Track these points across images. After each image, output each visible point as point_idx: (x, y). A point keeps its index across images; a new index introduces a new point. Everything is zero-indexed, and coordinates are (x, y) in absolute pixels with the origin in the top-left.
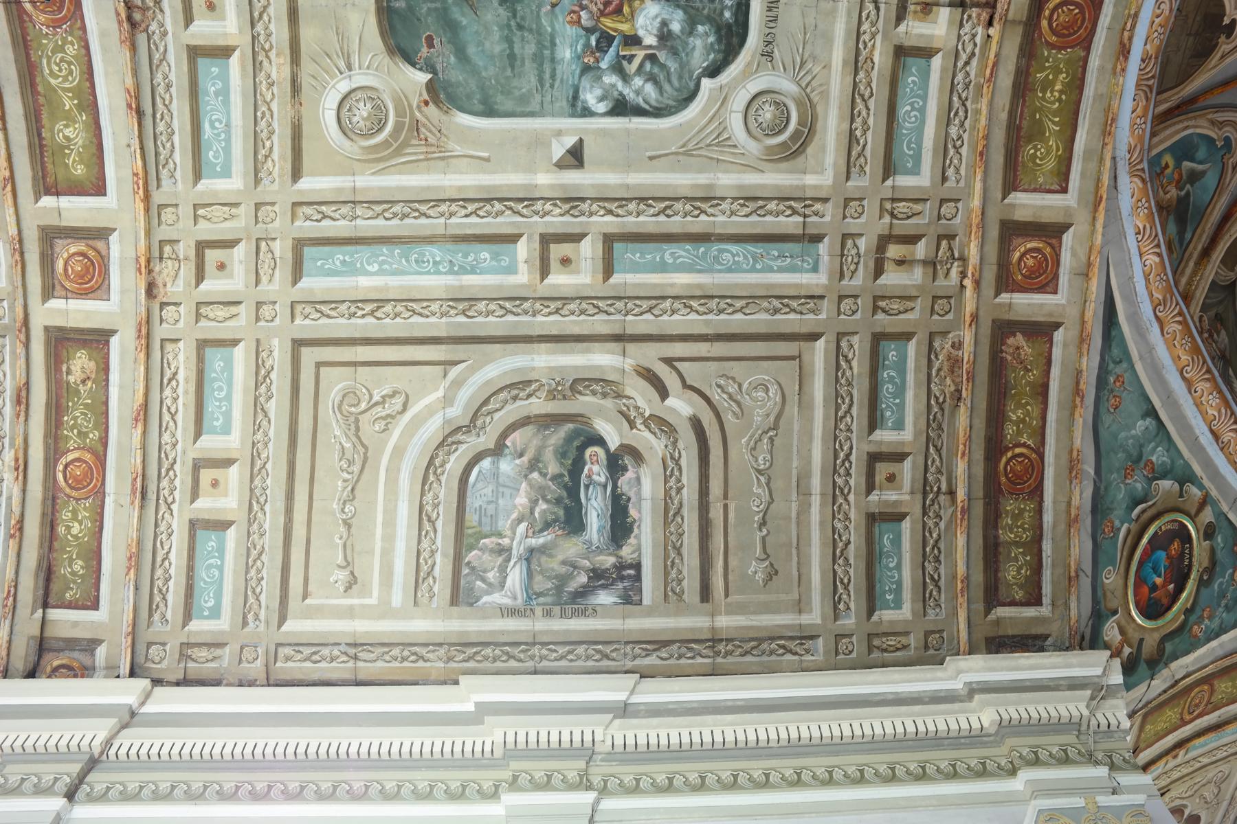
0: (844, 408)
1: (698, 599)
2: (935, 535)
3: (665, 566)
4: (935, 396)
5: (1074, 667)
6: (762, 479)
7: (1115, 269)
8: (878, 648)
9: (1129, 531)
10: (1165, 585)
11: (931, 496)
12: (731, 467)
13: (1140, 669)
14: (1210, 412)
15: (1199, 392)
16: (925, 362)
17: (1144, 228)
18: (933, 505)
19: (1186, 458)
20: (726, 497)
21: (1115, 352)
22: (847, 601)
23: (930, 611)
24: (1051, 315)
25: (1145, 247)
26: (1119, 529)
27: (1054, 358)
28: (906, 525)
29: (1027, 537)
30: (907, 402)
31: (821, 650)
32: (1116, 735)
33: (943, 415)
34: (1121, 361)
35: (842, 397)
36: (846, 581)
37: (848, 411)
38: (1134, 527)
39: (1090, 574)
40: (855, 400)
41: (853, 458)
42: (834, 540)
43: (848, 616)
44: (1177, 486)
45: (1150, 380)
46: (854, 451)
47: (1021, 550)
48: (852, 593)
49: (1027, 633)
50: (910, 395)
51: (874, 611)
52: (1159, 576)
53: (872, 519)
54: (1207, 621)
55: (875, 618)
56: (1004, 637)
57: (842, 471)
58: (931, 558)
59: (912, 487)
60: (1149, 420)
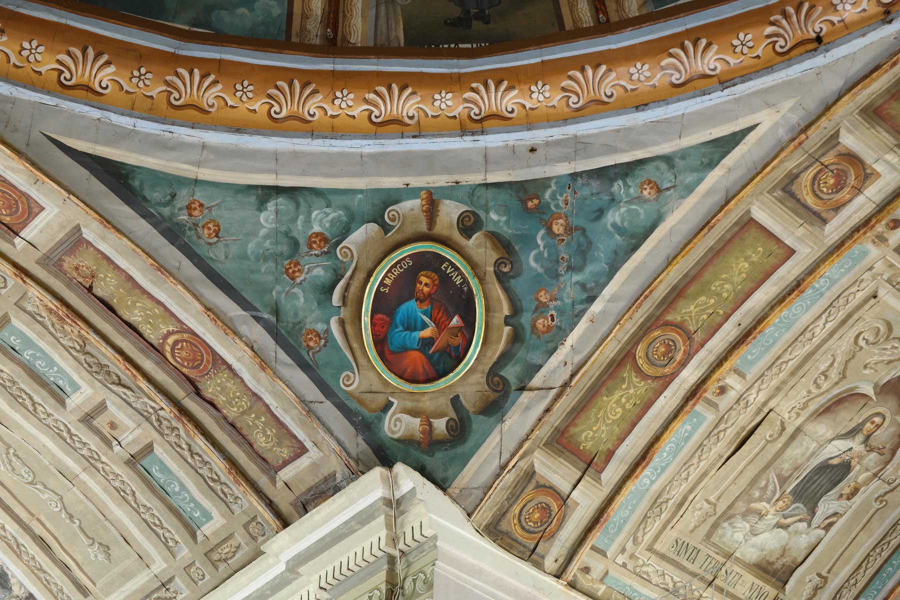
0: (28, 402)
1: (81, 597)
2: (184, 446)
3: (45, 585)
4: (72, 348)
5: (359, 500)
6: (38, 486)
7: (70, 136)
8: (220, 560)
9: (342, 323)
10: (440, 326)
11: (153, 418)
12: (15, 492)
13: (475, 426)
14: (355, 112)
15: (319, 114)
16: (38, 326)
17: (59, 62)
18: (161, 423)
19: (363, 187)
20: (32, 515)
21: (155, 195)
22: (172, 537)
23: (234, 507)
24: (62, 227)
25: (83, 75)
26: (328, 331)
27: (108, 254)
28: (158, 450)
29: (246, 403)
30: (61, 364)
31: (183, 586)
32: (426, 547)
33: (93, 356)
34: (173, 196)
35: (20, 397)
36: (157, 522)
37: (34, 403)
38: (345, 313)
39: (321, 397)
40: (28, 391)
41: (73, 431)
42: (123, 497)
43: (181, 549)
44: (373, 227)
45: (232, 170)
46: (69, 426)
47: (253, 416)
48: (170, 529)
49: (317, 480)
50: (56, 357)
51: (195, 533)
52: (425, 326)
53: (133, 461)
54: (552, 304)
55: (200, 538)
56: (301, 495)
57: (78, 445)
58: (199, 465)
59: (134, 421)
60: (271, 206)
